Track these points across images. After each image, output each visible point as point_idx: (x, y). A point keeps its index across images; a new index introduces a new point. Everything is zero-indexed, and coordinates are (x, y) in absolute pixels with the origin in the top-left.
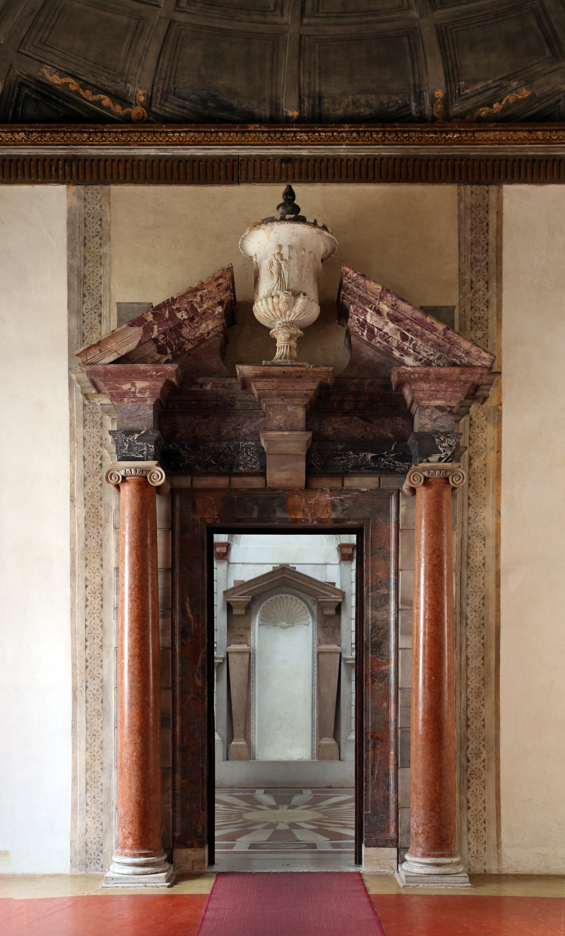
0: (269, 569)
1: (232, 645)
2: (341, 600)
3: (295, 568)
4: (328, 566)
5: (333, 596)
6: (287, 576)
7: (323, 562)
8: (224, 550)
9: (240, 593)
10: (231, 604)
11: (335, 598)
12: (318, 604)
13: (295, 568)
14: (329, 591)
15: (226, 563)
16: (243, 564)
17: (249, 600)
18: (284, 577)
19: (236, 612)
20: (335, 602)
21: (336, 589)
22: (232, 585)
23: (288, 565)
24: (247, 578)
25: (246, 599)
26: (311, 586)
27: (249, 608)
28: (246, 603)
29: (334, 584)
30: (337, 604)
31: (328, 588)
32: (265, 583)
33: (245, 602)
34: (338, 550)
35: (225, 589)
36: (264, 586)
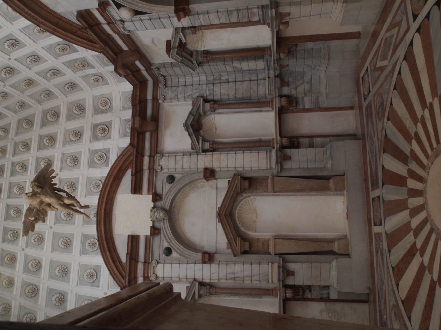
0: (220, 225)
1: (270, 251)
2: (239, 177)
3: (219, 207)
4: (218, 187)
5: (237, 181)
6: (224, 213)
7: (216, 190)
8: (207, 256)
9: (235, 245)
10: (242, 251)
11: (238, 181)
12: (242, 192)
13: (219, 207)
14: (234, 184)
15: (216, 255)
16: (216, 243)
17: (239, 238)
18: (225, 215)
19: (247, 248)
20: (240, 180)
21: (232, 180)
22: (230, 251)
23: (217, 212)
24: (226, 240)
25: (239, 240)
26: (230, 196)
27: (244, 239)
28: (242, 241)
29: (229, 181)
30: (242, 179)
31: (232, 185)
32: (228, 228)
33: (241, 242)
34: (208, 181)
35: (232, 256)
36: (230, 229)
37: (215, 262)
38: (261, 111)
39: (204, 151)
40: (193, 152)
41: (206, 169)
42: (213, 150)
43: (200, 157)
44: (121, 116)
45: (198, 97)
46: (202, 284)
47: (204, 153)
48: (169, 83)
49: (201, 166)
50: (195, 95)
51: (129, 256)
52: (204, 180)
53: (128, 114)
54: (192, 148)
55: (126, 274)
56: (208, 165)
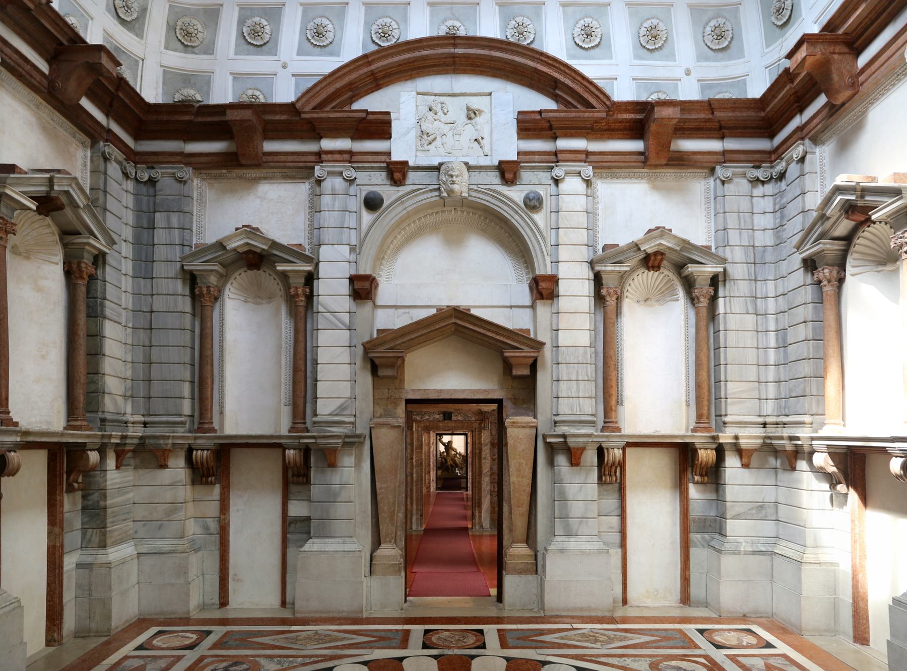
0: (433, 311)
37: (353, 304)
38: (688, 405)
39: (598, 279)
40: (595, 252)
41: (554, 280)
42: (599, 298)
43: (586, 267)
44: (685, 75)
45: (724, 261)
46: (310, 278)
47: (592, 276)
48: (759, 190)
49: (563, 271)
50: (727, 253)
51: (364, 115)
52: (531, 276)
53: (689, 92)
54: (605, 247)
55: (327, 112)
56: (563, 288)
